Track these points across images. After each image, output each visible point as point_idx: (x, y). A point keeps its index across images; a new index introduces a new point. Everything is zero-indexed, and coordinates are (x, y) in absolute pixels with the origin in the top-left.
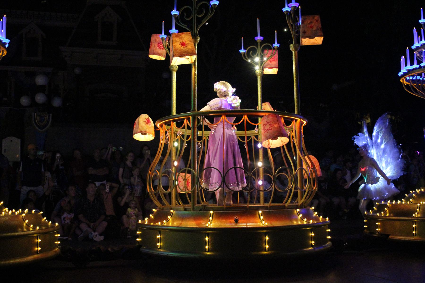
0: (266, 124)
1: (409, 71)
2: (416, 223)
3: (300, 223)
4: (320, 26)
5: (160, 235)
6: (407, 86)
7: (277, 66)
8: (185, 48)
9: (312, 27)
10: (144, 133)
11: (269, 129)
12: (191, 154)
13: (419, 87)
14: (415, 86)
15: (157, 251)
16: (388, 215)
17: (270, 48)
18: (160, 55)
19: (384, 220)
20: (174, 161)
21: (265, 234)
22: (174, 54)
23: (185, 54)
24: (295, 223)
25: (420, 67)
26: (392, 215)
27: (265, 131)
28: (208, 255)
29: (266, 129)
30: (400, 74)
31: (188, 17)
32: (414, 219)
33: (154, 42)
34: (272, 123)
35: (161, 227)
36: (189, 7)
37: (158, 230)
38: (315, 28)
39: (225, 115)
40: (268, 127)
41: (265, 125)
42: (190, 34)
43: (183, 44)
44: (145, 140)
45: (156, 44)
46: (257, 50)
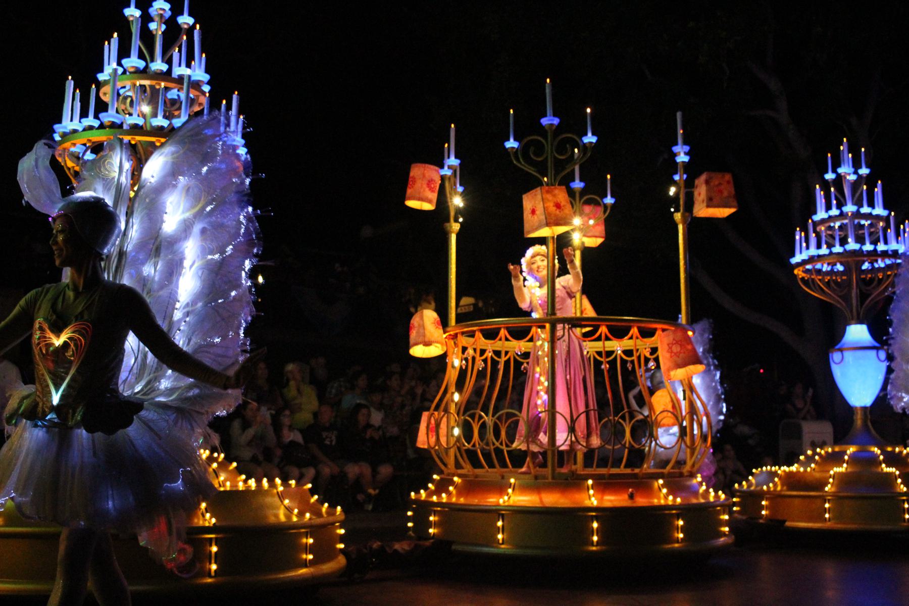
0: (673, 344)
1: (812, 259)
3: (702, 501)
4: (733, 192)
5: (503, 521)
7: (603, 234)
8: (562, 212)
9: (721, 192)
10: (427, 344)
11: (680, 353)
13: (828, 284)
16: (779, 488)
17: (597, 204)
18: (430, 201)
19: (774, 497)
20: (453, 393)
21: (678, 517)
24: (694, 501)
25: (831, 253)
26: (785, 488)
27: (673, 354)
28: (593, 551)
30: (794, 260)
31: (537, 155)
32: (827, 494)
34: (683, 343)
37: (497, 512)
38: (725, 194)
40: (676, 349)
42: (565, 190)
43: (558, 206)
44: (424, 356)
45: (425, 182)
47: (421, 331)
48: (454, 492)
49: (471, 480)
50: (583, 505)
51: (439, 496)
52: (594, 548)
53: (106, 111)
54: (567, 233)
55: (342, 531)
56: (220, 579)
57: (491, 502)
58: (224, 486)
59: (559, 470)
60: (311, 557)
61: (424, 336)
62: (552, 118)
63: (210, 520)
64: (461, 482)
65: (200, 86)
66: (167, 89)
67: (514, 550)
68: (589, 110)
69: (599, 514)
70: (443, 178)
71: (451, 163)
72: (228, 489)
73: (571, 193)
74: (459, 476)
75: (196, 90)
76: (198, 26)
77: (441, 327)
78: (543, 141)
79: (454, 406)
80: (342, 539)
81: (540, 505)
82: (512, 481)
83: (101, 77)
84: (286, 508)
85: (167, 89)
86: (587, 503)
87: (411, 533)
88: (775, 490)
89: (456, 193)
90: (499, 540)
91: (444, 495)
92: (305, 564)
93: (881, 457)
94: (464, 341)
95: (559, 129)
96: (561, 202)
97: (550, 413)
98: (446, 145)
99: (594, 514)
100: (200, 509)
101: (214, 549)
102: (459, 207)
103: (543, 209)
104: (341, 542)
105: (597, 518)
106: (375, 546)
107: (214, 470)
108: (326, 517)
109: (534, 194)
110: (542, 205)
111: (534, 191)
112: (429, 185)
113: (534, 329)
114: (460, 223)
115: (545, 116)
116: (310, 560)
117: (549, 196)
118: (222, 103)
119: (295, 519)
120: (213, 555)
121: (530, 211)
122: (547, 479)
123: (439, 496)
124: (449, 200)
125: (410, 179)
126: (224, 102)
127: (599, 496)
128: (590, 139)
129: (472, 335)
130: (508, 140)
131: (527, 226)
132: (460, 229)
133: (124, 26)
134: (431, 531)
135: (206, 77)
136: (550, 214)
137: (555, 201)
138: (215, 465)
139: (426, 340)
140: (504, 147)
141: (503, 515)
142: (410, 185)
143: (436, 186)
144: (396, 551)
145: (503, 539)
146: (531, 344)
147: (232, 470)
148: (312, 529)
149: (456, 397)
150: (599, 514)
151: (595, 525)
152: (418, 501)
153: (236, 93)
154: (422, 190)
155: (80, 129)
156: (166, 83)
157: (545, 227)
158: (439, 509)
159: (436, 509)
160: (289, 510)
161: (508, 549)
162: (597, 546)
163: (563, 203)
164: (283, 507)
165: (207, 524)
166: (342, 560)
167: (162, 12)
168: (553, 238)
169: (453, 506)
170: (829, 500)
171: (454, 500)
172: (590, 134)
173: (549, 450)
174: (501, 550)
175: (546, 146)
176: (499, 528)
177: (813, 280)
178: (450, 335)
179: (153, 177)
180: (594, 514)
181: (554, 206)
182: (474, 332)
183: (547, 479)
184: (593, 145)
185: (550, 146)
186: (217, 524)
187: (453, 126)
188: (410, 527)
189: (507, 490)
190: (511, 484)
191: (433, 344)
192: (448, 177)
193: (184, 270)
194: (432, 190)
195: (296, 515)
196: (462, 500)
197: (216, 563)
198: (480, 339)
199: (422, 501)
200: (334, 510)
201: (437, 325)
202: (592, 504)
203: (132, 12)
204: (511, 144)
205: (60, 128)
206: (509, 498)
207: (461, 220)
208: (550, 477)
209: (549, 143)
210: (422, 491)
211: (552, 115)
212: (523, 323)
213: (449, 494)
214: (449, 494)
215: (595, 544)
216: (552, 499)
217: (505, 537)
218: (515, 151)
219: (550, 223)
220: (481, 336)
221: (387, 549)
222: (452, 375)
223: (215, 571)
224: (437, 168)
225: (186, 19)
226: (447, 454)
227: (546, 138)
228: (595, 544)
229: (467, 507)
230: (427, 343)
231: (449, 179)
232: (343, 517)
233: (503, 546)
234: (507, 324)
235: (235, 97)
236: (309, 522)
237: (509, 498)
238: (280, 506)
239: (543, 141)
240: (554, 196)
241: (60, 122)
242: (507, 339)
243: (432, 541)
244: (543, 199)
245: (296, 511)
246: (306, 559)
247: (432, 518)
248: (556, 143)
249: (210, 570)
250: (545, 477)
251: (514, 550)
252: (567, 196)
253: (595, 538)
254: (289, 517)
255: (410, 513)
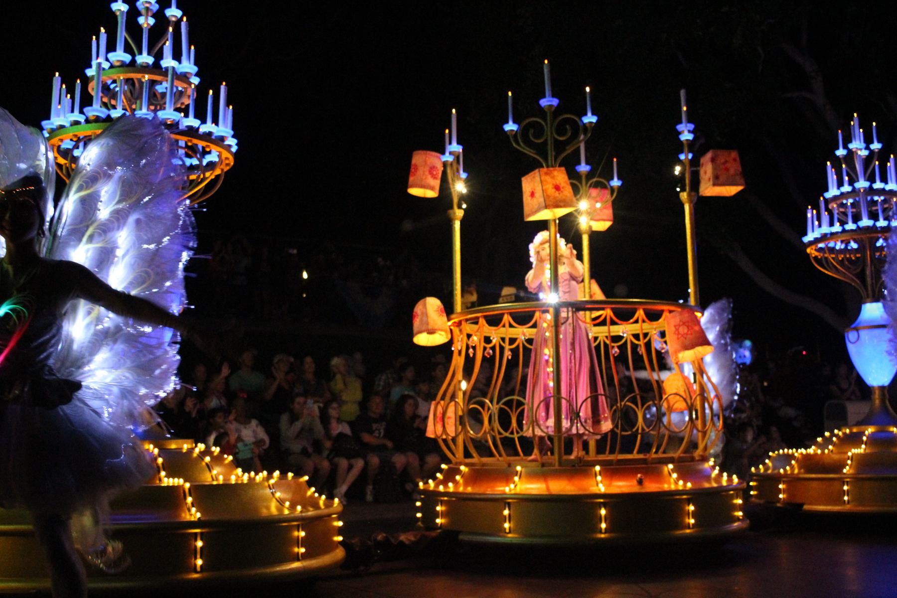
0: (679, 326)
1: (824, 238)
2: (849, 483)
3: (715, 485)
4: (740, 169)
5: (509, 510)
6: (816, 258)
7: (611, 217)
8: (561, 195)
9: (727, 169)
10: (431, 332)
11: (687, 334)
12: (584, 372)
13: (841, 263)
14: (833, 258)
15: (505, 537)
16: (796, 471)
17: (604, 187)
18: (432, 188)
19: (792, 480)
20: (460, 382)
21: (689, 502)
22: (547, 204)
23: (562, 204)
24: (707, 485)
25: (844, 231)
26: (802, 471)
27: (680, 336)
29: (682, 333)
30: (806, 239)
31: (537, 136)
33: (421, 166)
34: (690, 324)
35: (508, 496)
36: (539, 120)
37: (503, 501)
38: (732, 171)
39: (610, 308)
40: (683, 330)
41: (677, 327)
42: (565, 172)
43: (557, 188)
45: (427, 169)
46: (581, 188)
47: (425, 319)
48: (461, 481)
49: (478, 469)
50: (587, 492)
51: (446, 486)
52: (603, 536)
53: (91, 105)
54: (569, 215)
55: (340, 524)
56: (205, 574)
57: (499, 491)
58: (217, 480)
59: (565, 457)
60: (303, 550)
61: (428, 324)
62: (551, 99)
63: (195, 514)
64: (468, 472)
65: (188, 78)
66: (153, 83)
67: (521, 539)
68: (588, 89)
69: (607, 500)
70: (445, 164)
71: (452, 150)
72: (221, 482)
73: (573, 175)
74: (466, 465)
75: (184, 82)
76: (185, 19)
77: (445, 315)
78: (543, 123)
79: (462, 395)
80: (340, 531)
81: (545, 493)
82: (519, 468)
83: (90, 72)
84: (278, 501)
85: (153, 83)
86: (594, 490)
87: (420, 523)
88: (792, 473)
89: (459, 178)
90: (505, 529)
91: (450, 485)
92: (297, 558)
93: (160, 460)
94: (468, 328)
95: (557, 111)
96: (560, 184)
97: (556, 398)
98: (447, 131)
99: (602, 500)
100: (186, 504)
101: (200, 544)
102: (462, 193)
103: (541, 191)
104: (339, 535)
105: (604, 505)
106: (380, 537)
107: (207, 464)
108: (324, 509)
109: (532, 176)
110: (540, 188)
111: (532, 173)
112: (431, 172)
113: (537, 314)
114: (464, 209)
115: (544, 96)
116: (302, 554)
117: (548, 178)
118: (208, 93)
119: (286, 512)
120: (199, 550)
121: (530, 194)
122: (554, 466)
123: (446, 486)
124: (451, 186)
125: (412, 167)
126: (211, 92)
127: (607, 482)
128: (590, 119)
129: (475, 322)
130: (507, 122)
131: (527, 209)
132: (464, 216)
133: (111, 20)
134: (438, 521)
135: (193, 69)
136: (548, 196)
137: (554, 182)
138: (208, 459)
139: (430, 327)
140: (503, 129)
141: (509, 504)
142: (413, 173)
143: (439, 173)
144: (401, 542)
145: (510, 528)
146: (534, 330)
147: (228, 464)
148: (305, 523)
149: (464, 385)
150: (607, 500)
151: (603, 512)
152: (426, 492)
153: (224, 83)
154: (424, 177)
155: (67, 124)
156: (150, 75)
157: (544, 209)
158: (446, 498)
159: (442, 498)
160: (281, 502)
161: (516, 538)
162: (605, 533)
163: (562, 185)
164: (274, 500)
165: (193, 519)
166: (339, 554)
167: (148, 5)
168: (555, 221)
169: (462, 496)
170: (847, 482)
171: (461, 489)
172: (589, 114)
173: (555, 436)
174: (507, 539)
175: (545, 127)
176: (505, 516)
177: (826, 258)
178: (454, 322)
179: (89, 165)
180: (602, 500)
181: (553, 188)
182: (478, 318)
183: (554, 466)
184: (593, 125)
185: (549, 129)
186: (201, 519)
187: (454, 111)
188: (419, 518)
189: (513, 478)
190: (517, 472)
191: (437, 332)
192: (449, 163)
193: (116, 259)
194: (435, 177)
195: (287, 508)
196: (469, 489)
197: (201, 558)
198: (484, 325)
199: (431, 491)
200: (331, 501)
201: (440, 313)
202: (600, 490)
203: (120, 7)
204: (510, 127)
205: (47, 124)
206: (516, 486)
207: (464, 206)
208: (557, 464)
209: (549, 125)
210: (430, 481)
211: (551, 96)
212: (528, 308)
213: (456, 483)
214: (456, 483)
215: (603, 531)
216: (560, 486)
217: (512, 526)
218: (515, 134)
219: (549, 206)
220: (484, 322)
221: (393, 541)
222: (458, 362)
223: (201, 566)
224: (438, 155)
225: (174, 11)
226: (455, 444)
227: (545, 120)
228: (603, 531)
229: (473, 496)
230: (432, 331)
231: (451, 164)
232: (340, 509)
233: (510, 535)
234: (511, 309)
235: (223, 88)
236: (300, 515)
237: (516, 486)
238: (272, 498)
239: (543, 123)
240: (553, 177)
241: (48, 118)
242: (511, 326)
243: (439, 531)
244: (541, 181)
245: (287, 504)
246: (298, 553)
247: (439, 508)
248: (555, 124)
249: (195, 565)
250: (551, 465)
251: (521, 539)
252: (566, 177)
253: (603, 526)
254: (280, 510)
255: (418, 504)
